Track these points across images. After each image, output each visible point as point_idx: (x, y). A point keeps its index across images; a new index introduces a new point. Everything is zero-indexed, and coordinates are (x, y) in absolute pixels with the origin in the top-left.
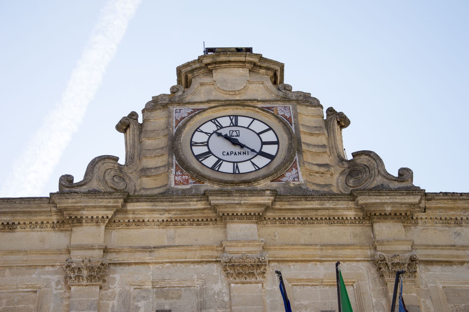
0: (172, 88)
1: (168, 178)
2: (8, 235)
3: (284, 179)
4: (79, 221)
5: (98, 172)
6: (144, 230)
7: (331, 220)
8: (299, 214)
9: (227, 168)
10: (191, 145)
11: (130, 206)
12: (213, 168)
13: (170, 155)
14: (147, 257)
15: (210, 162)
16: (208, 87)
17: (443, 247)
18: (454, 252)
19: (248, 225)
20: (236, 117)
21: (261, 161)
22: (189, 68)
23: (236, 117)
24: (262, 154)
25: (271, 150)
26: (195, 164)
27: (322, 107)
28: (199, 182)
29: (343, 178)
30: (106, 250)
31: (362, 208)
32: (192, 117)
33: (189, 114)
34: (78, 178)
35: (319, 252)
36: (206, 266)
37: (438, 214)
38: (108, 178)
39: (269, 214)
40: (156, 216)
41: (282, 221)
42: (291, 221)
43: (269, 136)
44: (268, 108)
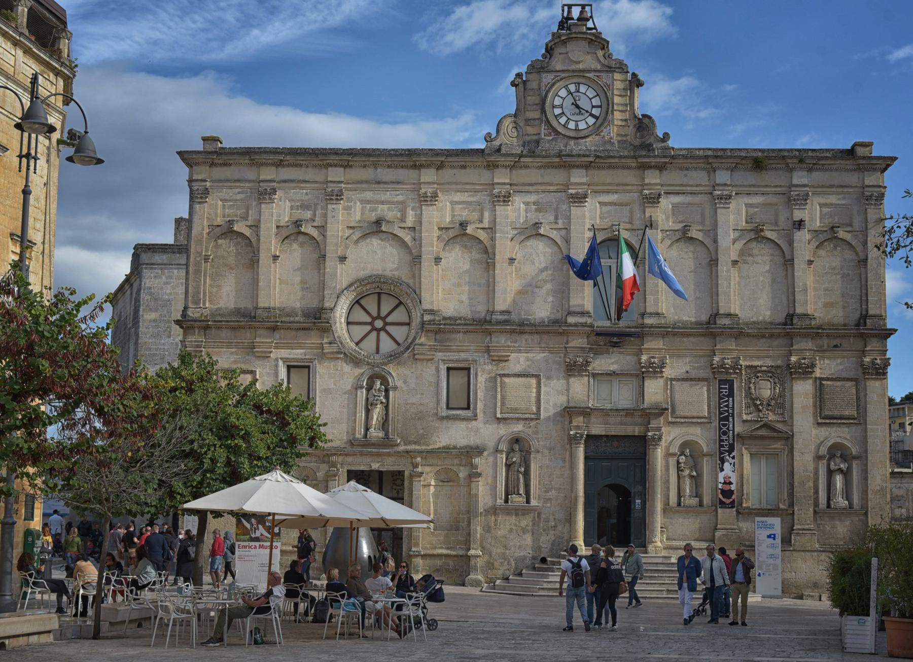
0: (543, 55)
1: (541, 131)
2: (464, 170)
3: (602, 134)
4: (497, 166)
5: (504, 128)
6: (529, 170)
7: (623, 168)
8: (608, 165)
9: (572, 125)
10: (553, 107)
11: (522, 160)
12: (564, 126)
13: (542, 113)
14: (530, 188)
15: (563, 120)
16: (563, 55)
17: (676, 185)
18: (682, 188)
19: (581, 170)
20: (579, 84)
21: (591, 121)
22: (553, 43)
23: (579, 84)
24: (592, 115)
25: (596, 111)
26: (554, 123)
27: (628, 72)
28: (557, 134)
29: (635, 130)
30: (511, 185)
31: (637, 162)
32: (553, 85)
33: (552, 80)
34: (494, 135)
35: (615, 188)
36: (559, 194)
37: (678, 165)
38: (509, 130)
39: (593, 164)
40: (535, 164)
41: (599, 168)
42: (603, 168)
43: (596, 102)
44: (598, 76)
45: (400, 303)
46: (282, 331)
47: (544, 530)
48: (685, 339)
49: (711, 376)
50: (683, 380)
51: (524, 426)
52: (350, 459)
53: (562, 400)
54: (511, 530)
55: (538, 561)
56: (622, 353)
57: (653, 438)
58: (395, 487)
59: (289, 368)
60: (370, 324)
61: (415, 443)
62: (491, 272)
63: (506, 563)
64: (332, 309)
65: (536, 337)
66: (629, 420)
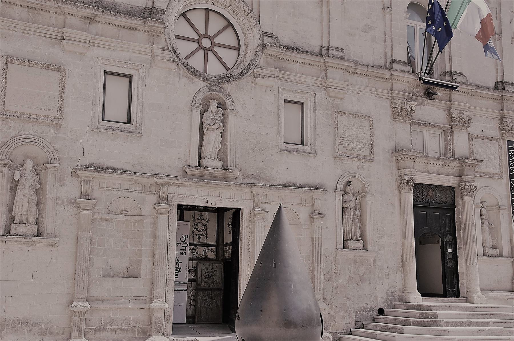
45: (230, 24)
46: (100, 25)
47: (379, 279)
48: (479, 101)
49: (499, 136)
50: (481, 138)
51: (358, 168)
52: (182, 191)
53: (390, 145)
54: (350, 279)
55: (376, 312)
56: (433, 106)
57: (470, 188)
58: (196, 232)
59: (106, 73)
60: (198, 41)
61: (254, 177)
62: (325, 8)
63: (347, 315)
64: (163, 12)
65: (365, 80)
66: (444, 170)
